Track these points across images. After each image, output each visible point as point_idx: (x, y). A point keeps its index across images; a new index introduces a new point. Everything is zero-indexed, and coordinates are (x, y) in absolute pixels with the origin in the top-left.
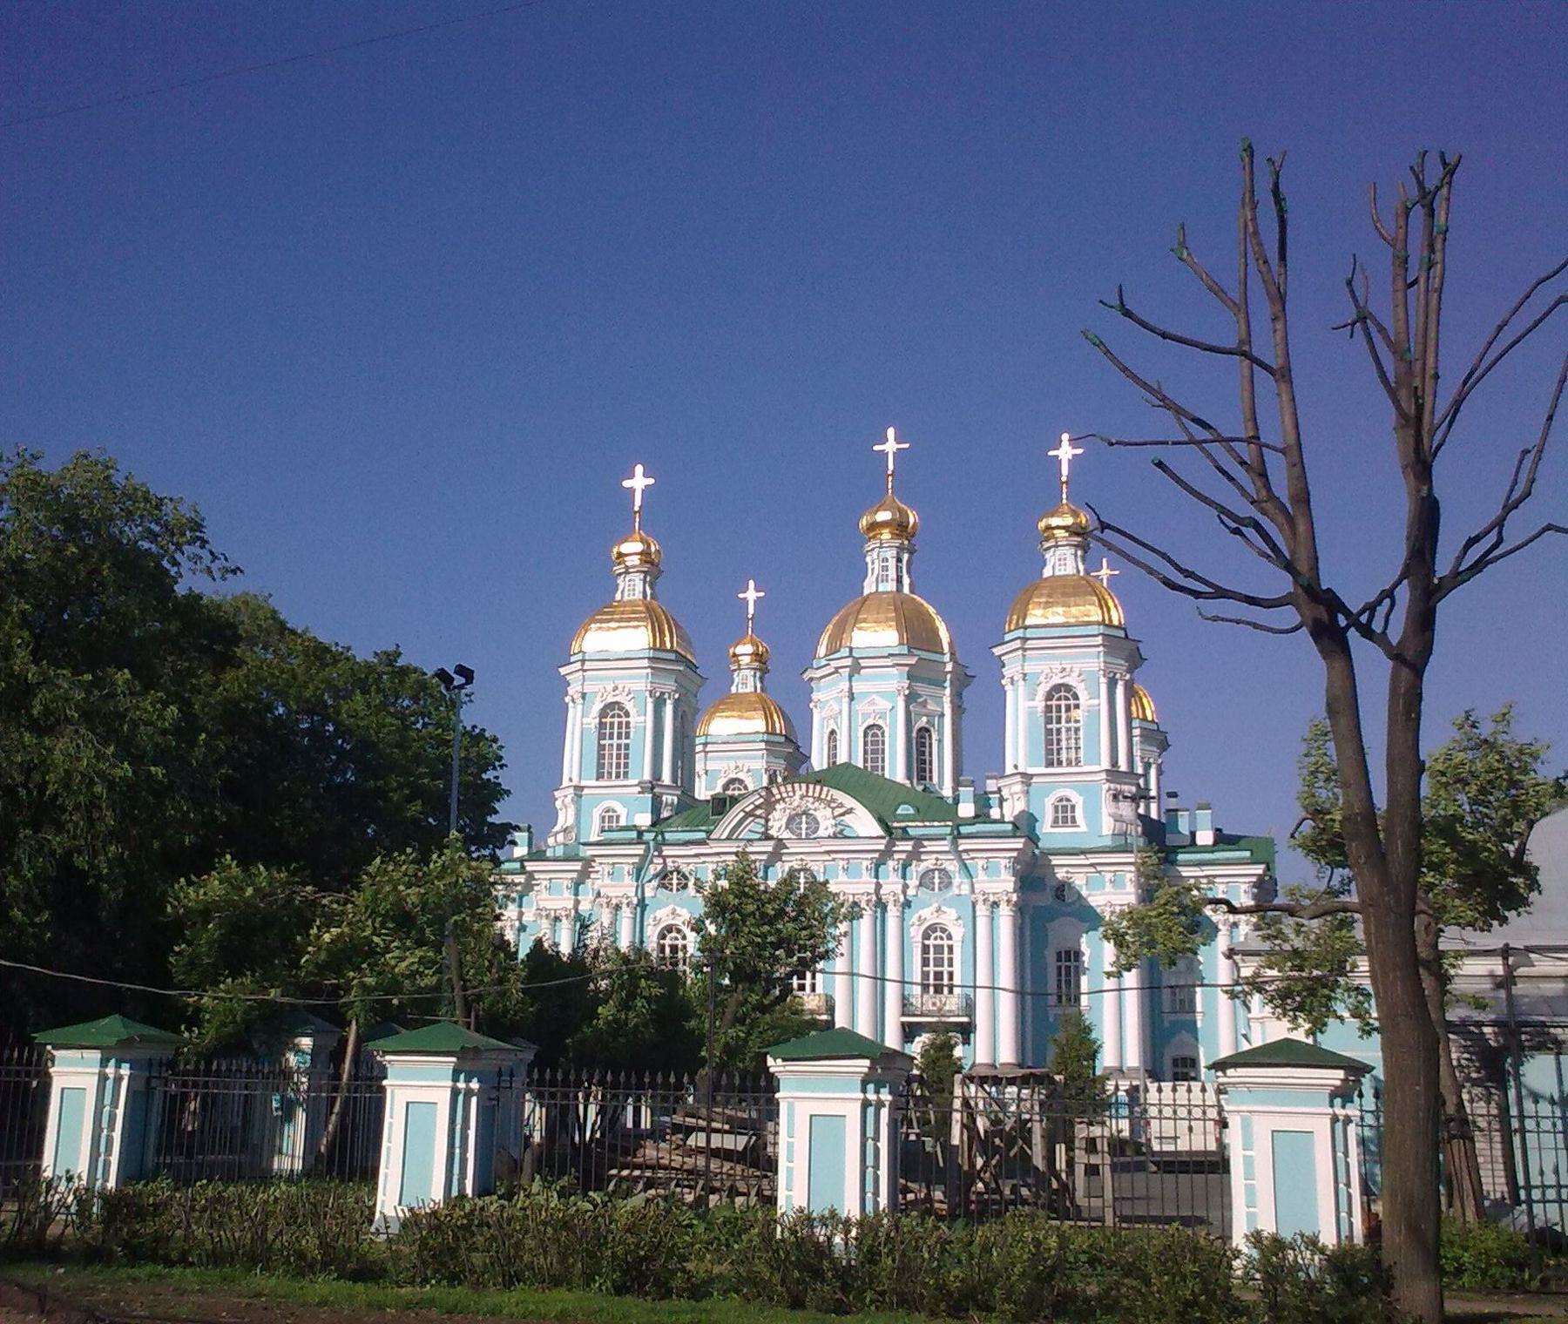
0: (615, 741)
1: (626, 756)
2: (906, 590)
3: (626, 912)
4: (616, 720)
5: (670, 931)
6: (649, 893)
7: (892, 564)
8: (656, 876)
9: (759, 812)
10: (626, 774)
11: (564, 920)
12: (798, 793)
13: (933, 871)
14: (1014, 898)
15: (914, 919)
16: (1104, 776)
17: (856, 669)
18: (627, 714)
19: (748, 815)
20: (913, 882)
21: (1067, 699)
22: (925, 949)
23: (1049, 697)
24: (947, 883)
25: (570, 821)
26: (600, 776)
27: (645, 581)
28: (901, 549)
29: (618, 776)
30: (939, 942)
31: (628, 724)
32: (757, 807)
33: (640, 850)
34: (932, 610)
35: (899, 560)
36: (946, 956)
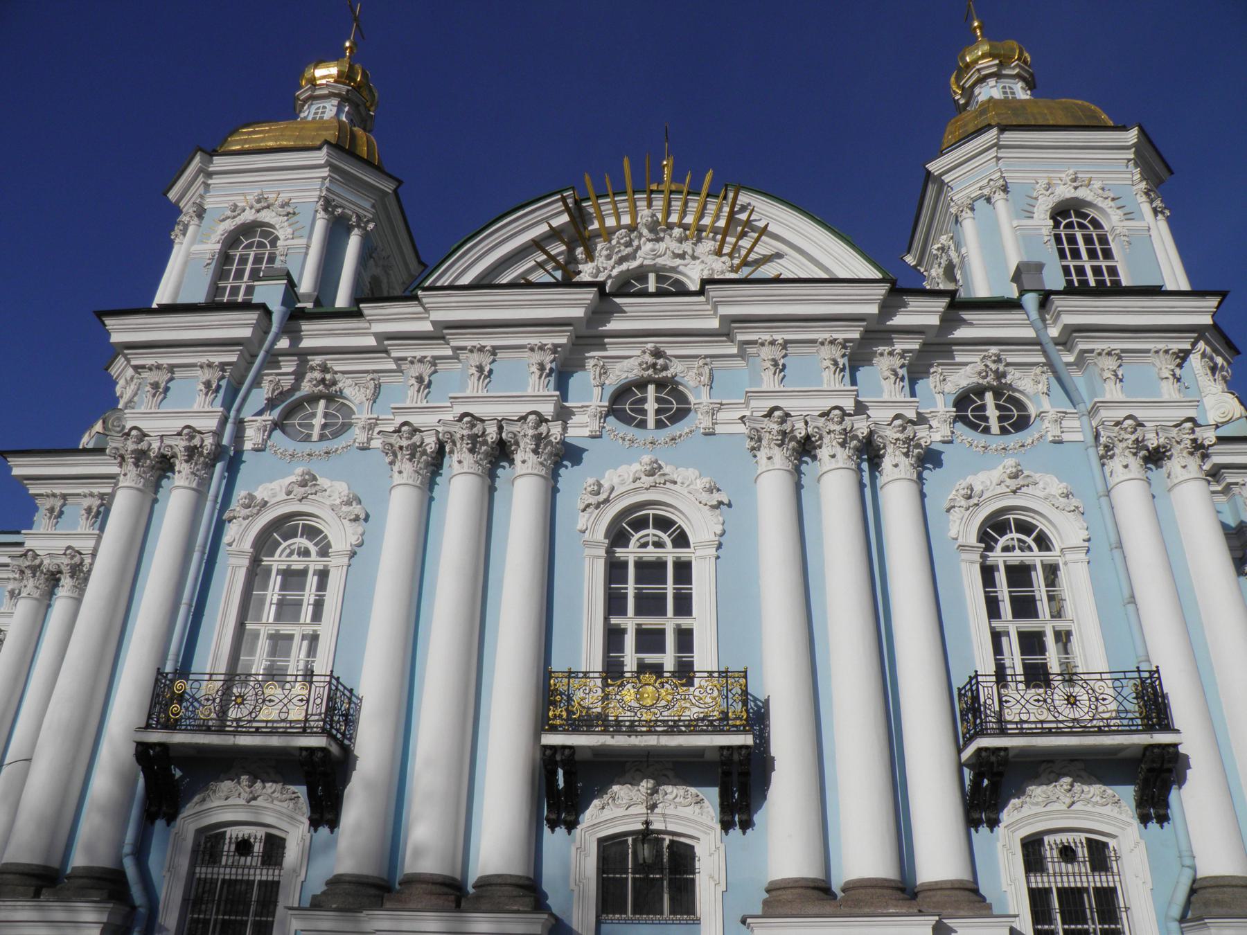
6: (252, 436)
20: (942, 408)
21: (1081, 226)
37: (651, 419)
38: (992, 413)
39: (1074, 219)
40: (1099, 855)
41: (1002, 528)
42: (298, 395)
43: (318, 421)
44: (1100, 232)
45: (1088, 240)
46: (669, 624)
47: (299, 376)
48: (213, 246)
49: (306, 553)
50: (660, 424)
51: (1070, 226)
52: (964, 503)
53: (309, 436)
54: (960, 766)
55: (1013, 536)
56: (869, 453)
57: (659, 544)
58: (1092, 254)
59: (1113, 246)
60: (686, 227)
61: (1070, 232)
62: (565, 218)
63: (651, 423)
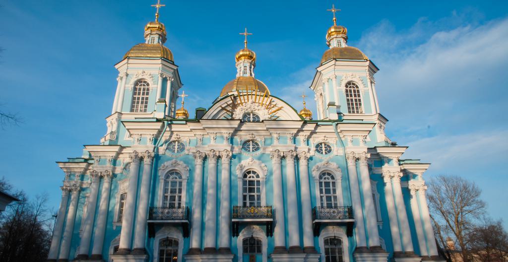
0: (141, 96)
4: (142, 87)
5: (172, 174)
7: (248, 68)
8: (166, 142)
9: (229, 109)
10: (145, 111)
11: (106, 177)
12: (250, 101)
14: (369, 156)
15: (314, 167)
18: (148, 85)
19: (223, 109)
20: (313, 148)
21: (353, 87)
22: (321, 183)
23: (346, 86)
25: (114, 129)
27: (159, 38)
28: (251, 63)
30: (327, 180)
31: (148, 90)
32: (228, 105)
34: (263, 83)
35: (250, 68)
36: (331, 187)
37: (251, 149)
38: (324, 149)
39: (352, 85)
41: (324, 174)
42: (171, 140)
43: (176, 147)
46: (255, 194)
47: (171, 137)
48: (131, 86)
49: (176, 178)
50: (253, 151)
51: (350, 87)
52: (317, 170)
53: (174, 151)
54: (313, 224)
55: (327, 176)
56: (297, 158)
57: (253, 177)
58: (355, 96)
59: (361, 93)
60: (260, 103)
61: (350, 89)
62: (231, 102)
63: (251, 151)
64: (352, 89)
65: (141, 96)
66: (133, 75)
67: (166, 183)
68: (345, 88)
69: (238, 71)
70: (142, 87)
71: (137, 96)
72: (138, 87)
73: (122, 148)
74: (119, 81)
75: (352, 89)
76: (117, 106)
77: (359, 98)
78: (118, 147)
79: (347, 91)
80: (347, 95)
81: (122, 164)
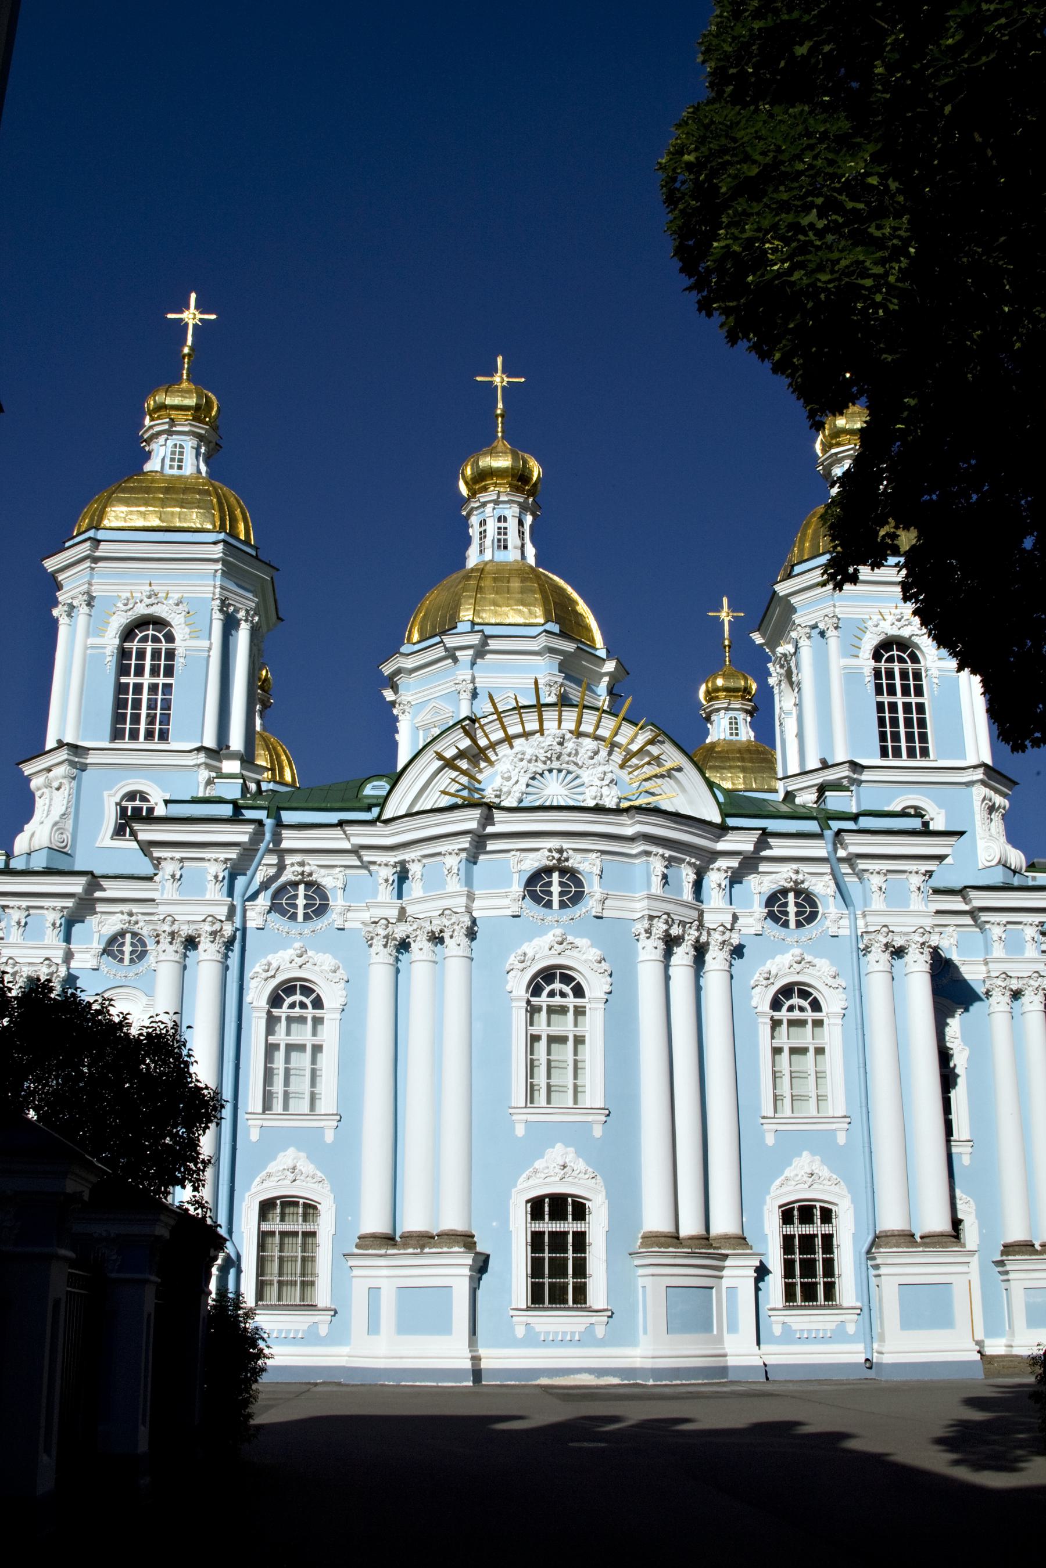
0: (146, 680)
1: (167, 705)
2: (531, 560)
3: (208, 951)
6: (255, 918)
7: (512, 525)
13: (784, 892)
16: (979, 775)
17: (480, 652)
21: (901, 660)
23: (877, 656)
24: (809, 909)
26: (117, 734)
29: (149, 735)
31: (171, 655)
33: (241, 834)
35: (521, 523)
39: (895, 653)
40: (827, 1216)
42: (283, 879)
44: (916, 666)
45: (904, 675)
51: (890, 659)
55: (795, 1001)
64: (896, 667)
65: (146, 680)
66: (112, 601)
67: (272, 1022)
68: (872, 663)
69: (474, 532)
70: (149, 647)
71: (131, 680)
72: (134, 646)
73: (94, 880)
74: (63, 621)
75: (896, 667)
76: (63, 722)
77: (919, 700)
78: (83, 880)
79: (877, 674)
80: (879, 691)
81: (96, 936)
